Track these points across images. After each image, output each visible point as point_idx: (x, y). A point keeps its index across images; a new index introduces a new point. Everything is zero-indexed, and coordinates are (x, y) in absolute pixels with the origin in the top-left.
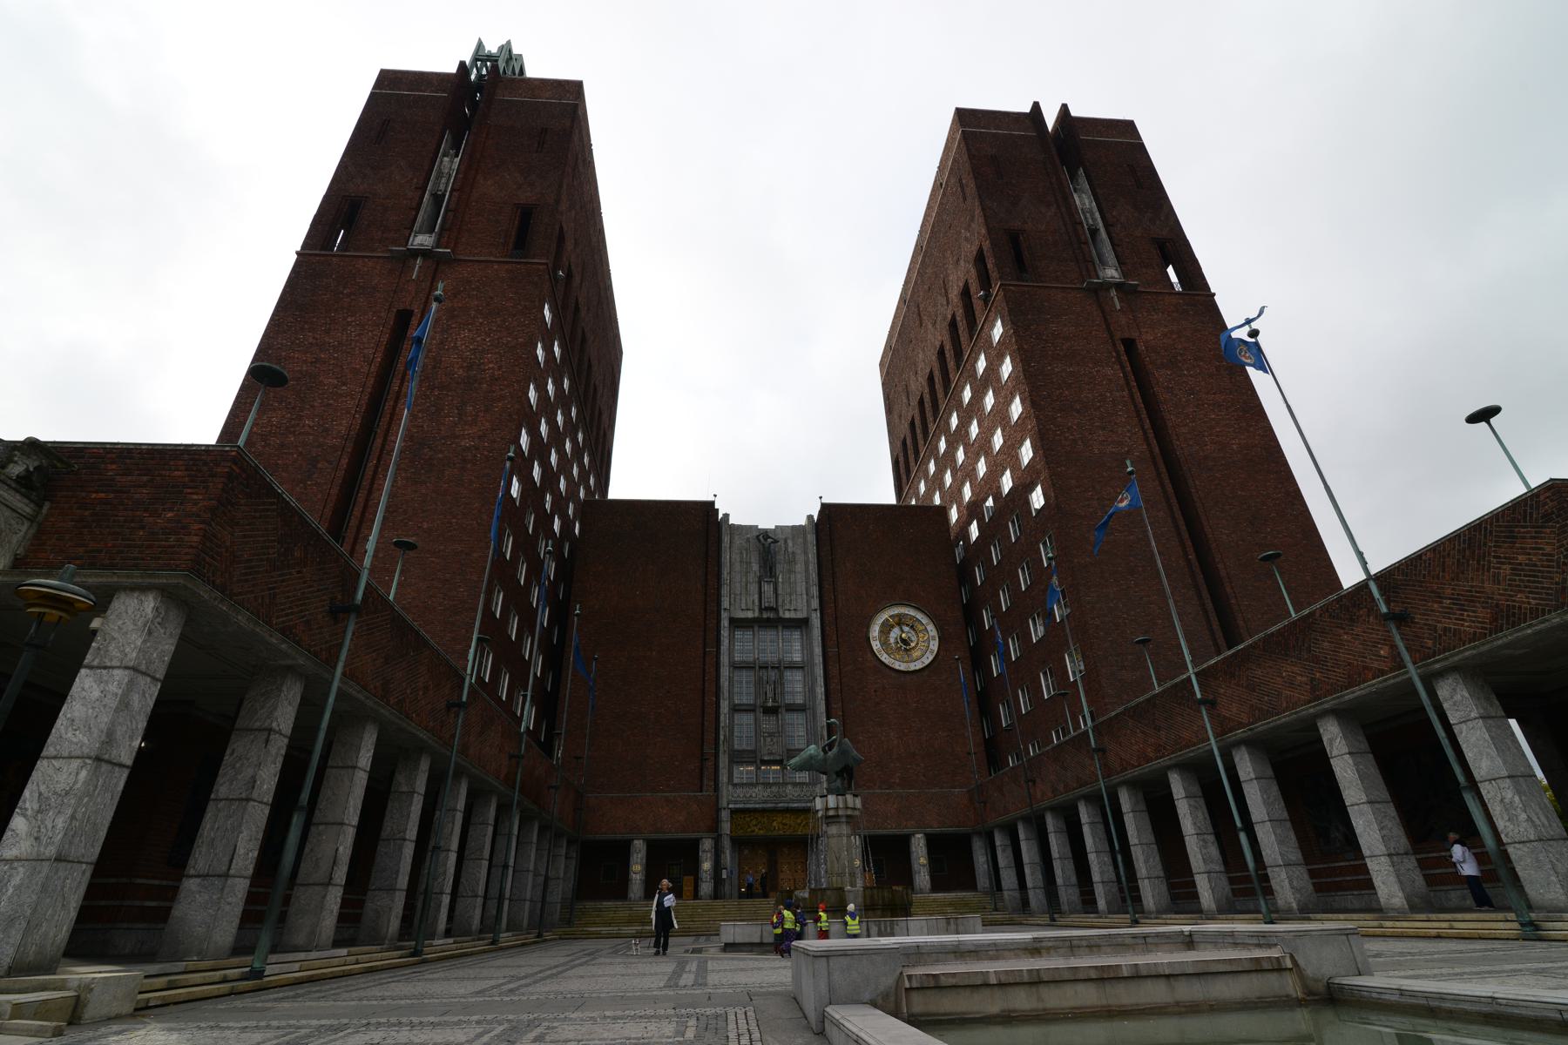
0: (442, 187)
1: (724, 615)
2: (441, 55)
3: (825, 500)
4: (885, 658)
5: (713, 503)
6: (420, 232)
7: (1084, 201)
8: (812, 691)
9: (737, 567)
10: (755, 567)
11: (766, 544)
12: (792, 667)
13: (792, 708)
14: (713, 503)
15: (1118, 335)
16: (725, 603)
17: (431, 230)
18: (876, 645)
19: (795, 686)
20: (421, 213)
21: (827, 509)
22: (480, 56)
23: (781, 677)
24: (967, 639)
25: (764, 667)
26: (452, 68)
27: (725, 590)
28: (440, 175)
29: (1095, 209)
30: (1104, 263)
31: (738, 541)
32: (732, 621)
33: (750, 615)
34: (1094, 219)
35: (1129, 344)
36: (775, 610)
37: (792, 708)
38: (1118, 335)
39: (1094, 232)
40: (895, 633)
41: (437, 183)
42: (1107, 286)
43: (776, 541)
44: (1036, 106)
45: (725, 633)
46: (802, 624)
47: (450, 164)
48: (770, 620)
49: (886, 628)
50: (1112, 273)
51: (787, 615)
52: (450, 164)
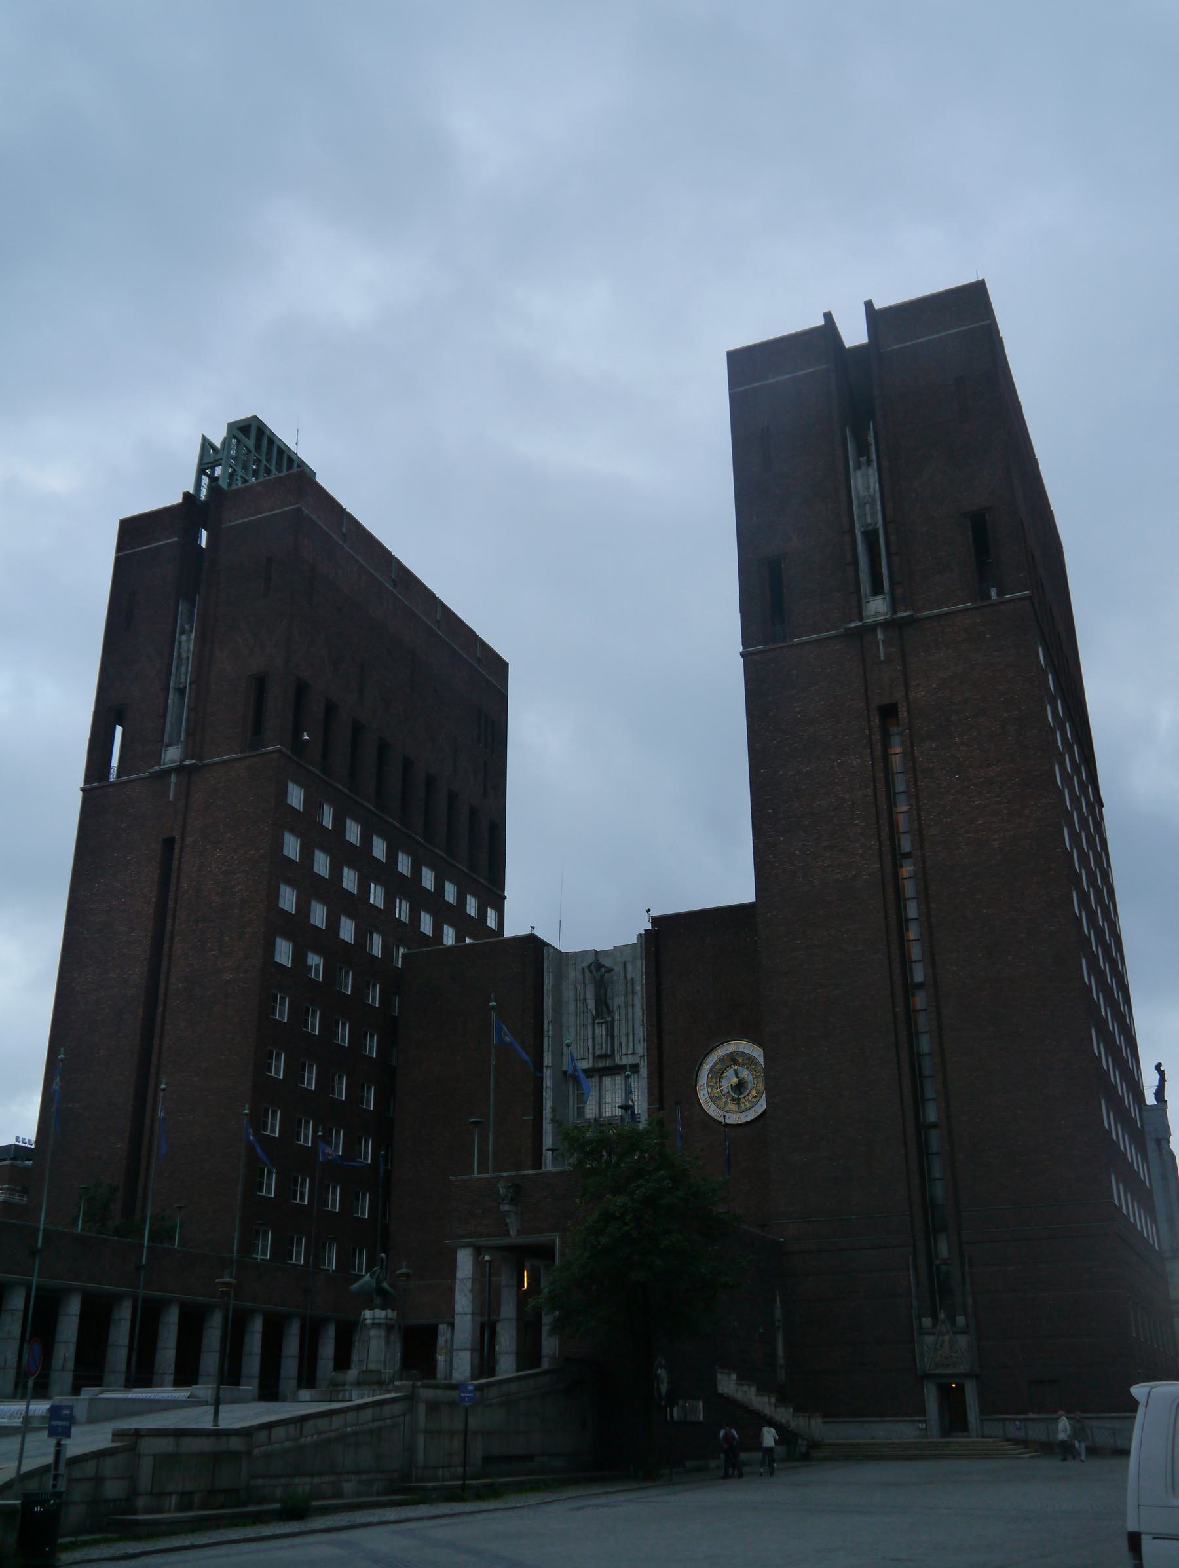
0: (183, 680)
2: (169, 484)
3: (653, 914)
4: (713, 1111)
6: (169, 745)
7: (865, 483)
9: (572, 1007)
10: (591, 1004)
16: (547, 1059)
17: (178, 742)
18: (703, 1095)
20: (169, 719)
21: (656, 921)
22: (209, 456)
26: (179, 499)
29: (878, 495)
31: (572, 974)
34: (874, 514)
36: (612, 1056)
41: (178, 675)
42: (872, 628)
43: (610, 970)
44: (828, 316)
46: (635, 1068)
49: (717, 1074)
52: (187, 644)
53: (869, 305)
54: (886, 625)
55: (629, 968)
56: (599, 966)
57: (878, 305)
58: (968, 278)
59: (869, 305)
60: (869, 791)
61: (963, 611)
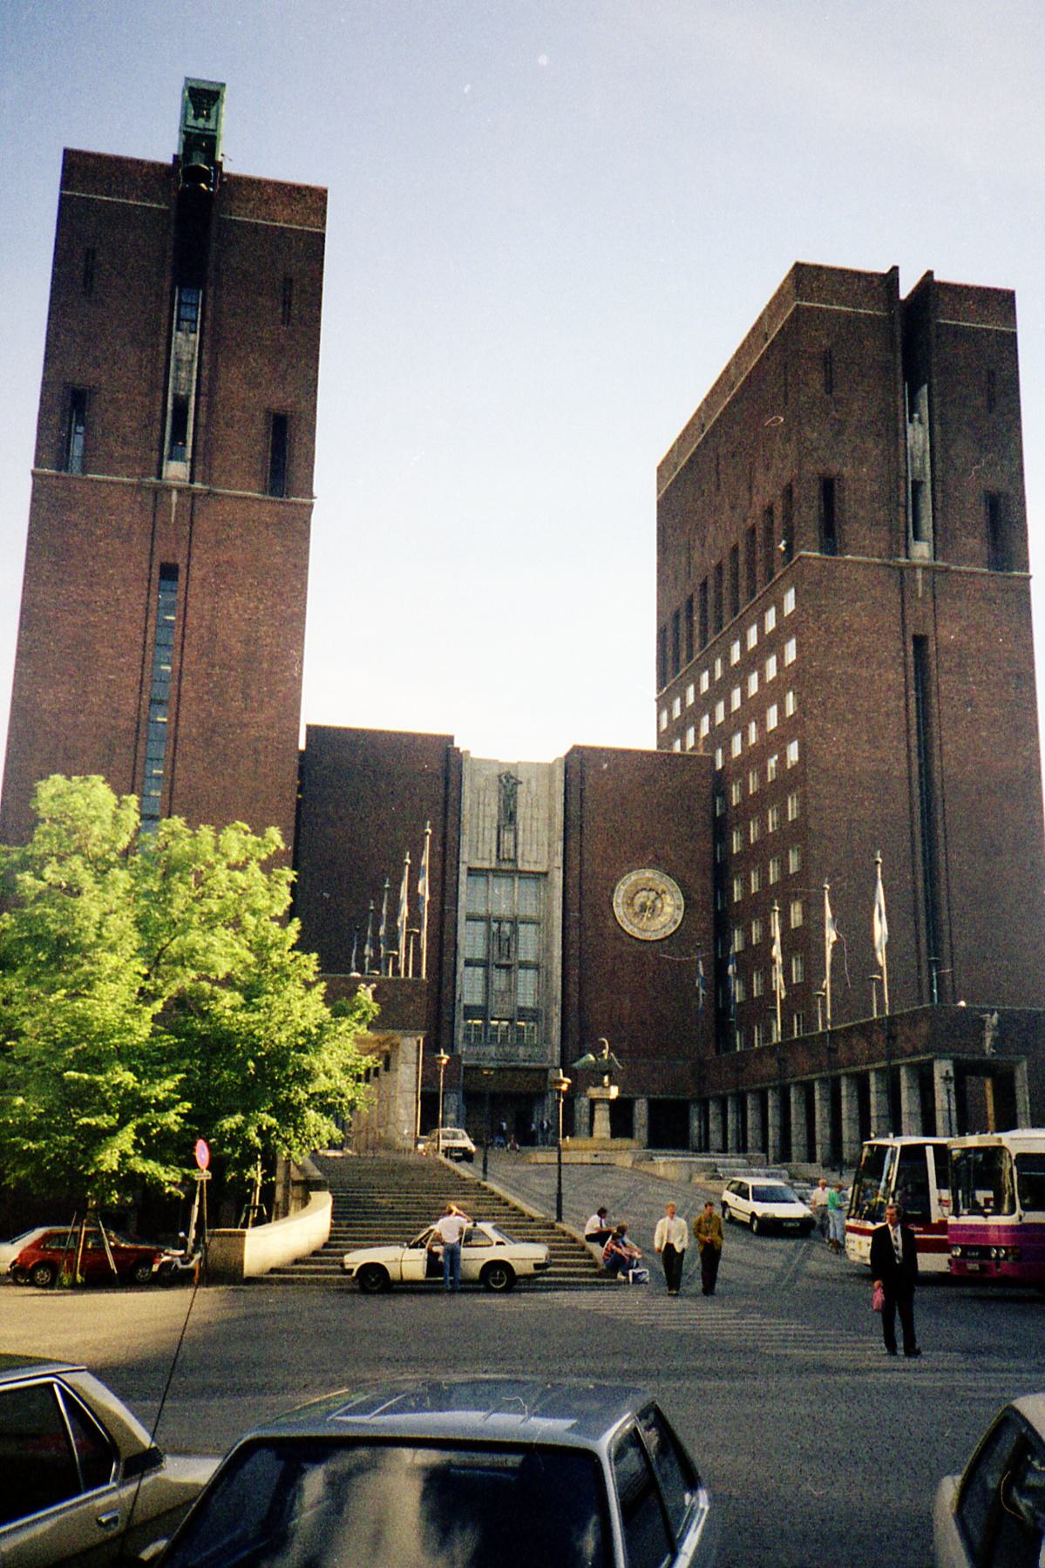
1: (463, 868)
5: (451, 739)
7: (917, 436)
8: (548, 949)
11: (508, 783)
12: (527, 921)
13: (524, 965)
14: (451, 739)
15: (911, 630)
16: (464, 856)
18: (619, 911)
19: (528, 945)
23: (515, 931)
24: (716, 913)
25: (499, 921)
27: (465, 839)
28: (178, 360)
30: (917, 538)
32: (472, 872)
33: (486, 865)
35: (920, 642)
36: (514, 861)
37: (524, 965)
38: (911, 630)
39: (917, 485)
40: (641, 898)
44: (895, 269)
45: (462, 888)
47: (186, 344)
48: (507, 869)
50: (922, 551)
51: (527, 867)
53: (930, 274)
54: (925, 568)
55: (533, 784)
56: (509, 777)
57: (937, 278)
58: (1010, 288)
59: (930, 274)
60: (902, 703)
61: (983, 575)
